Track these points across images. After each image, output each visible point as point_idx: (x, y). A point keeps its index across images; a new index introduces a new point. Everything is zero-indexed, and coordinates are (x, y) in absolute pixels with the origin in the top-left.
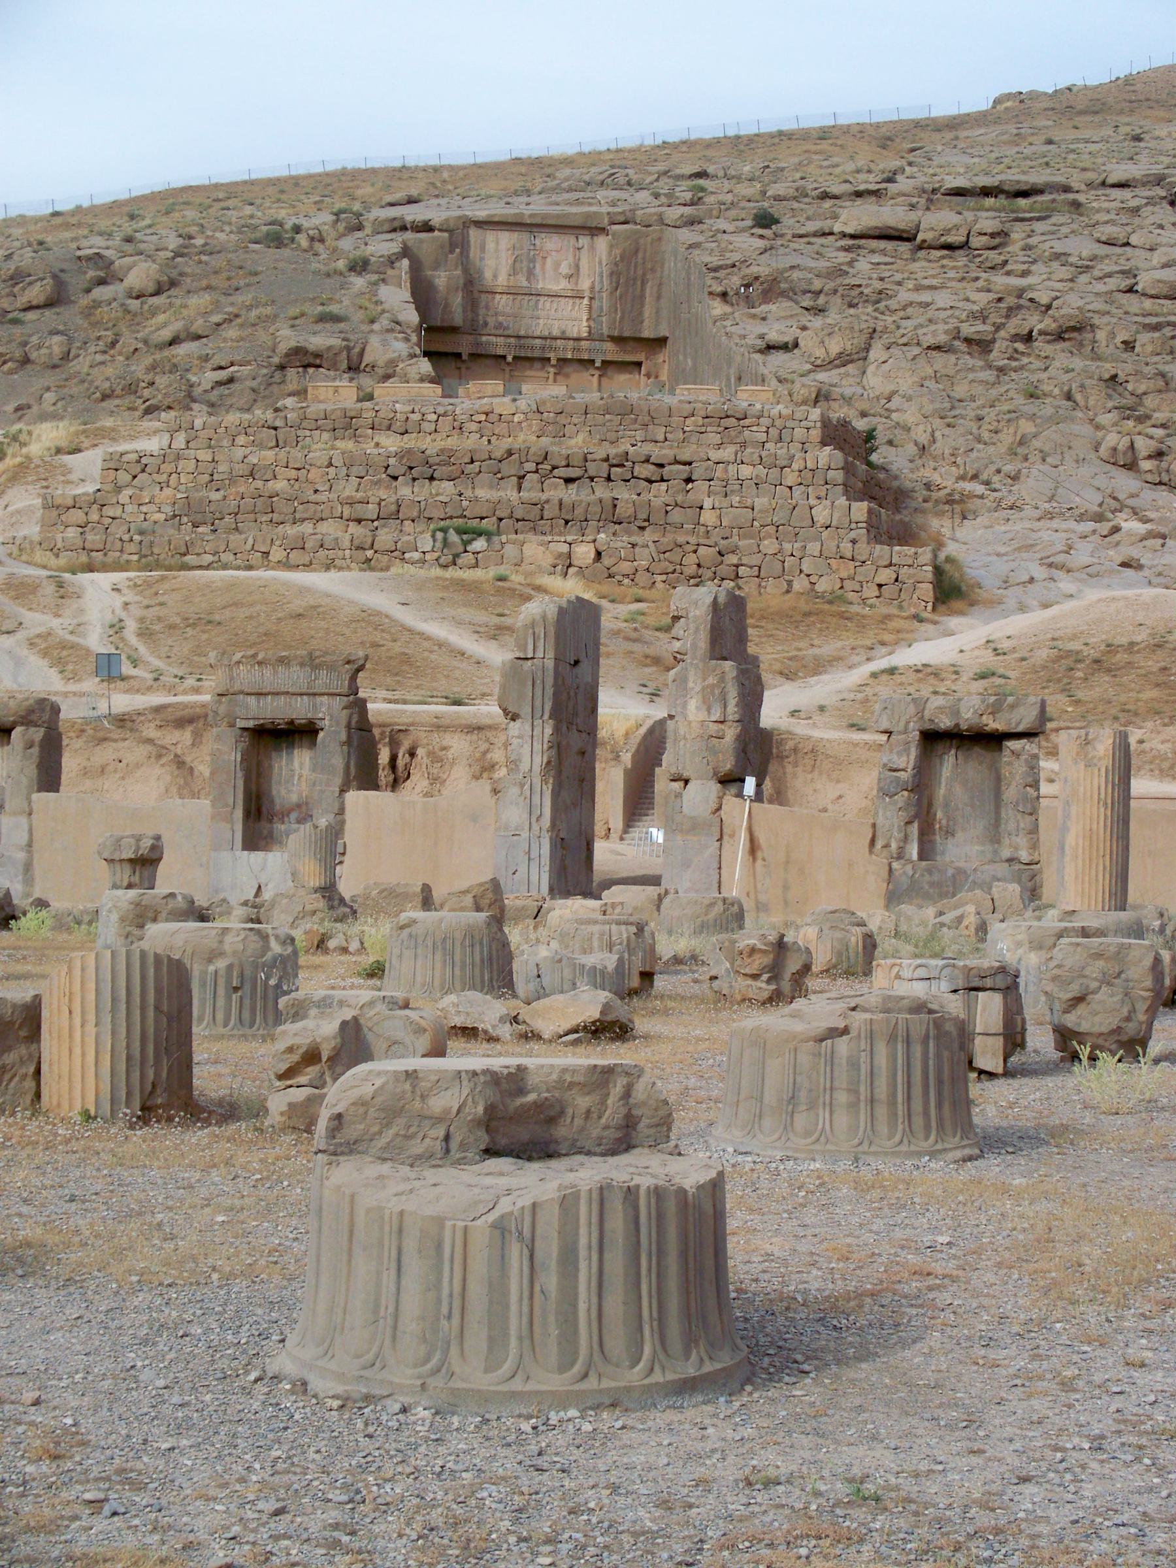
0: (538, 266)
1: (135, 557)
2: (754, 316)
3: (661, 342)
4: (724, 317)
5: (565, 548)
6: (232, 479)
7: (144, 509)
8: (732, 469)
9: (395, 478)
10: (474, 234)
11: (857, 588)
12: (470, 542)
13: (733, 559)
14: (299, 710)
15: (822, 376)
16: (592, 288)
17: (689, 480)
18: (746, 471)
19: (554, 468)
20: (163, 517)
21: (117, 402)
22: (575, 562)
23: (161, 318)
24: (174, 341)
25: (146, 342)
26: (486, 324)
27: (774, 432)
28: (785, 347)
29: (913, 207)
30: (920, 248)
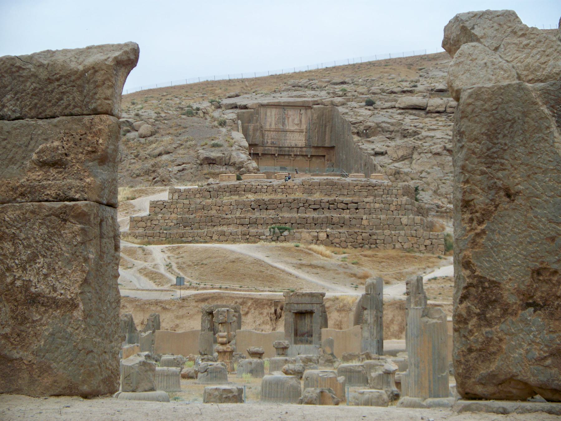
0: (286, 121)
1: (164, 239)
2: (369, 141)
3: (333, 148)
4: (358, 141)
5: (316, 234)
6: (197, 210)
7: (166, 221)
8: (372, 205)
9: (254, 209)
10: (262, 110)
11: (418, 246)
12: (283, 232)
13: (375, 237)
14: (308, 308)
15: (396, 164)
16: (306, 129)
17: (357, 209)
18: (377, 205)
19: (310, 205)
20: (173, 224)
21: (142, 178)
22: (320, 239)
23: (154, 146)
24: (160, 155)
25: (149, 155)
26: (267, 142)
27: (386, 191)
28: (382, 154)
29: (424, 97)
30: (428, 113)
